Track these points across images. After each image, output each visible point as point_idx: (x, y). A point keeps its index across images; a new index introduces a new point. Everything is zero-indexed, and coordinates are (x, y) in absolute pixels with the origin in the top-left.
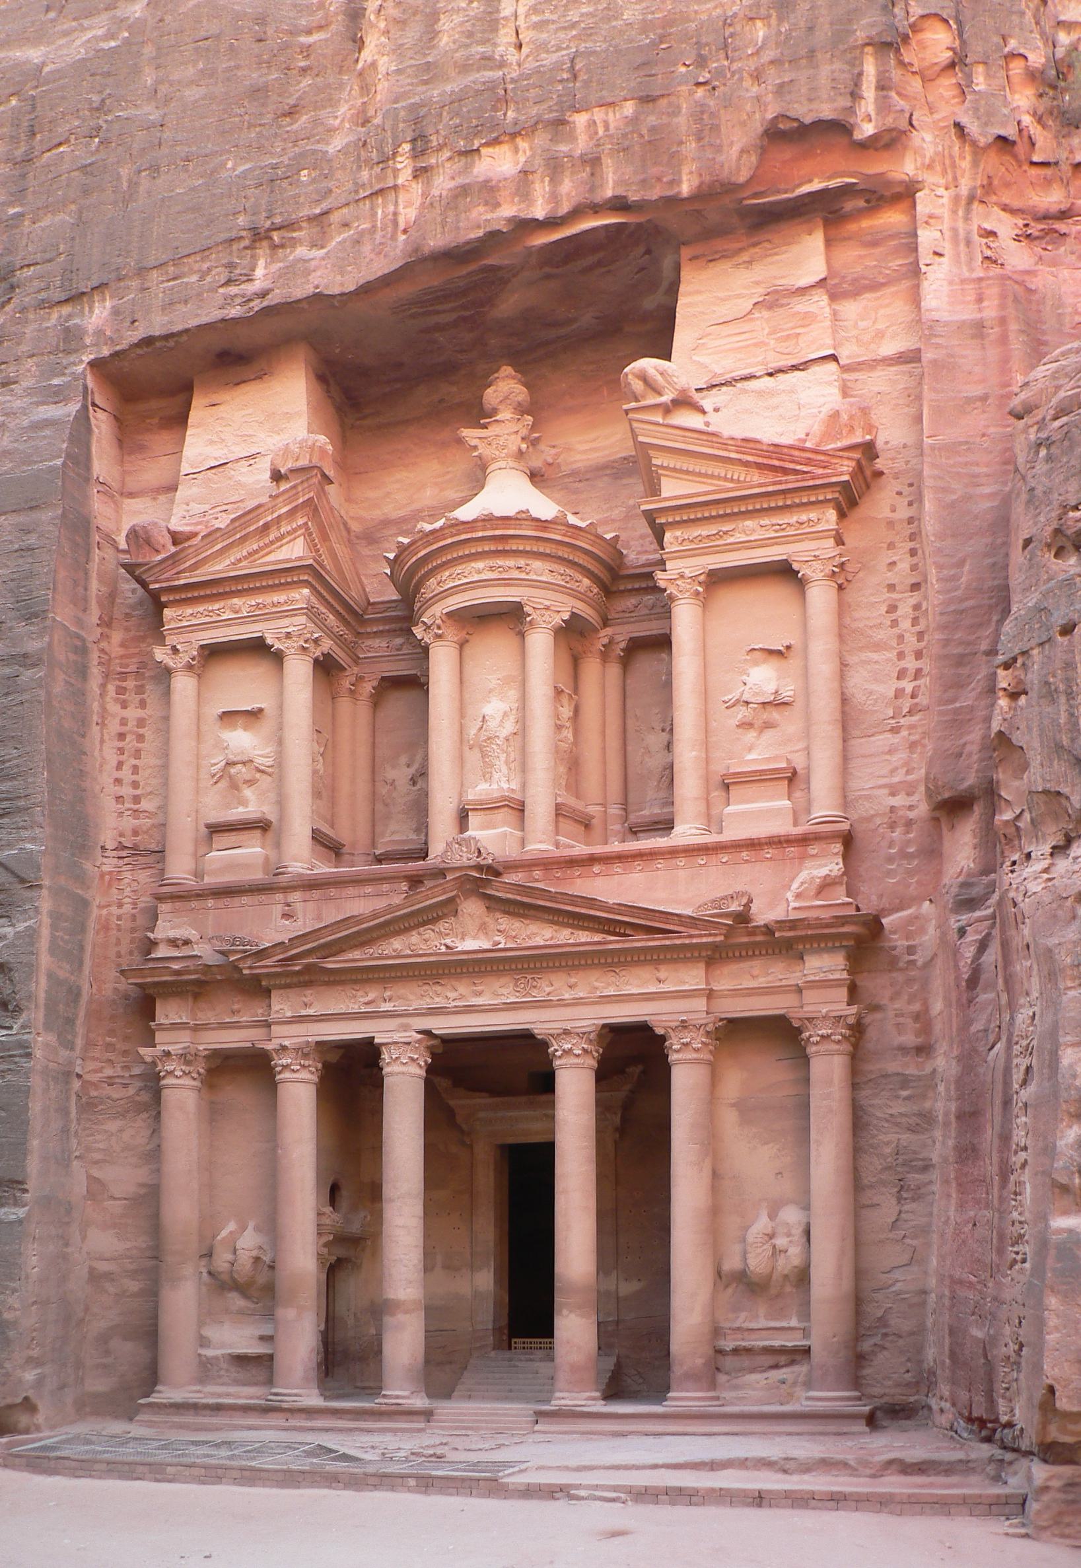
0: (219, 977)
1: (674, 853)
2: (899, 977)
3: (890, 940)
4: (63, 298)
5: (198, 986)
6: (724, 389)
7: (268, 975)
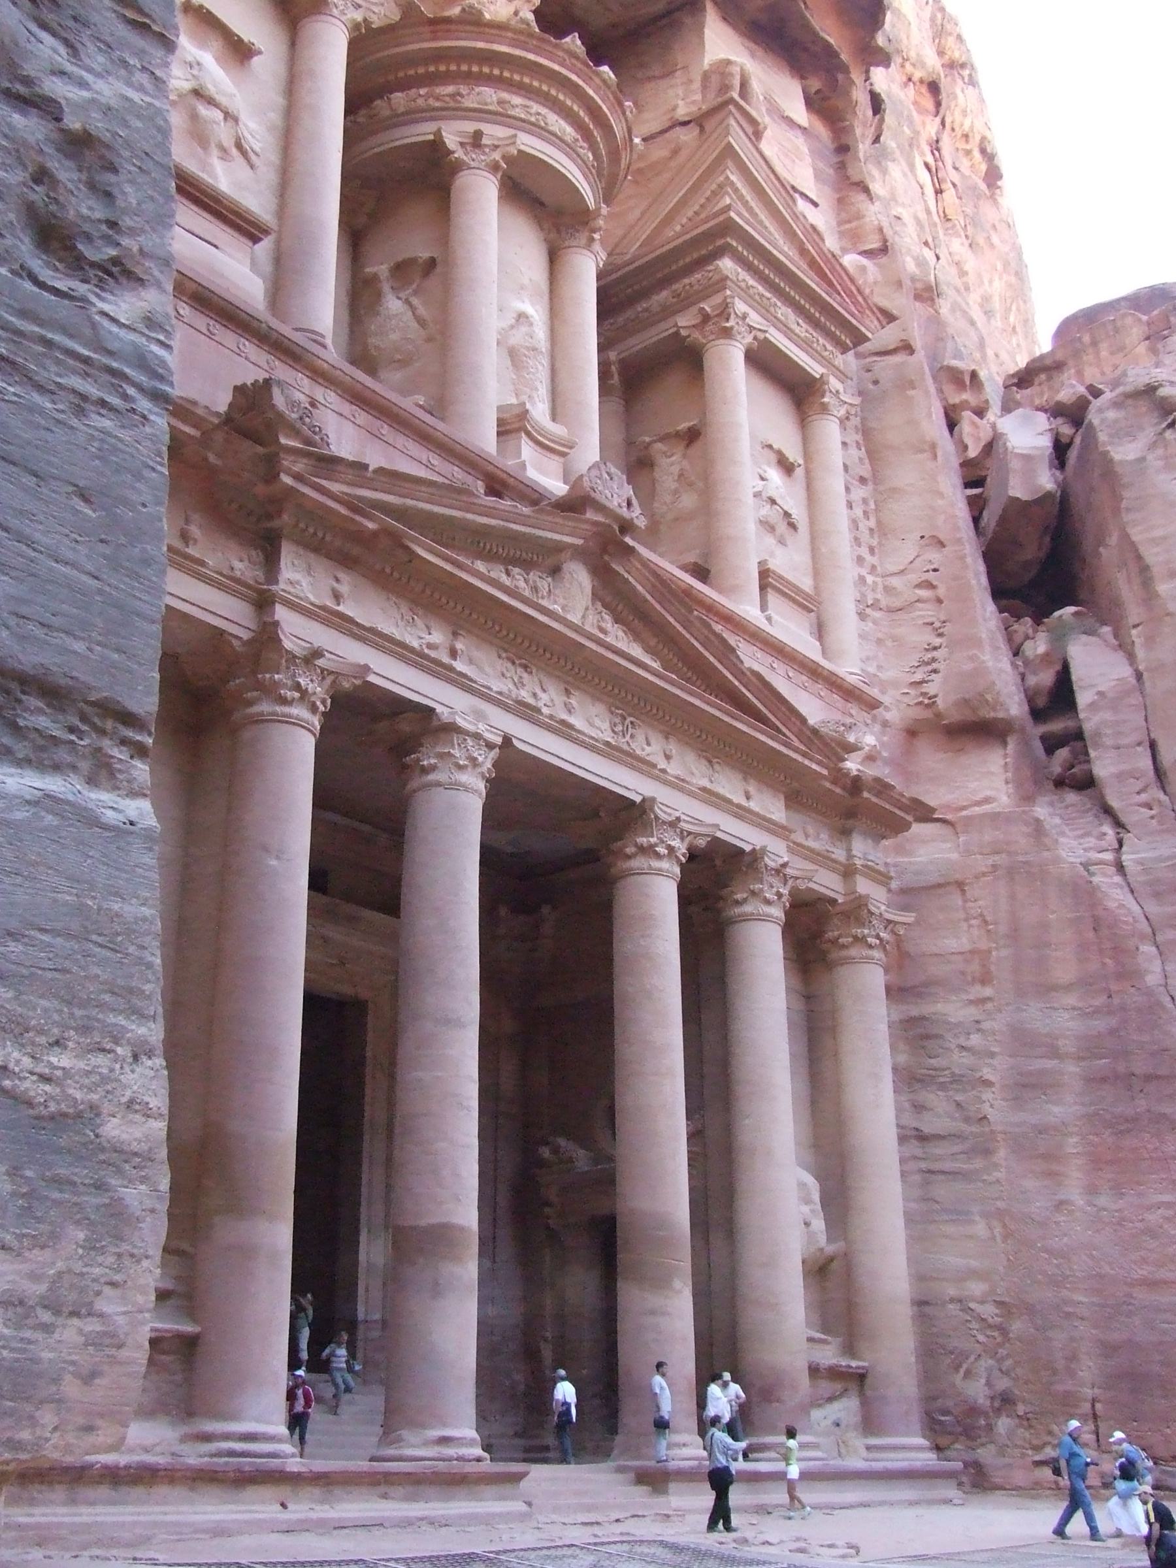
0: (212, 458)
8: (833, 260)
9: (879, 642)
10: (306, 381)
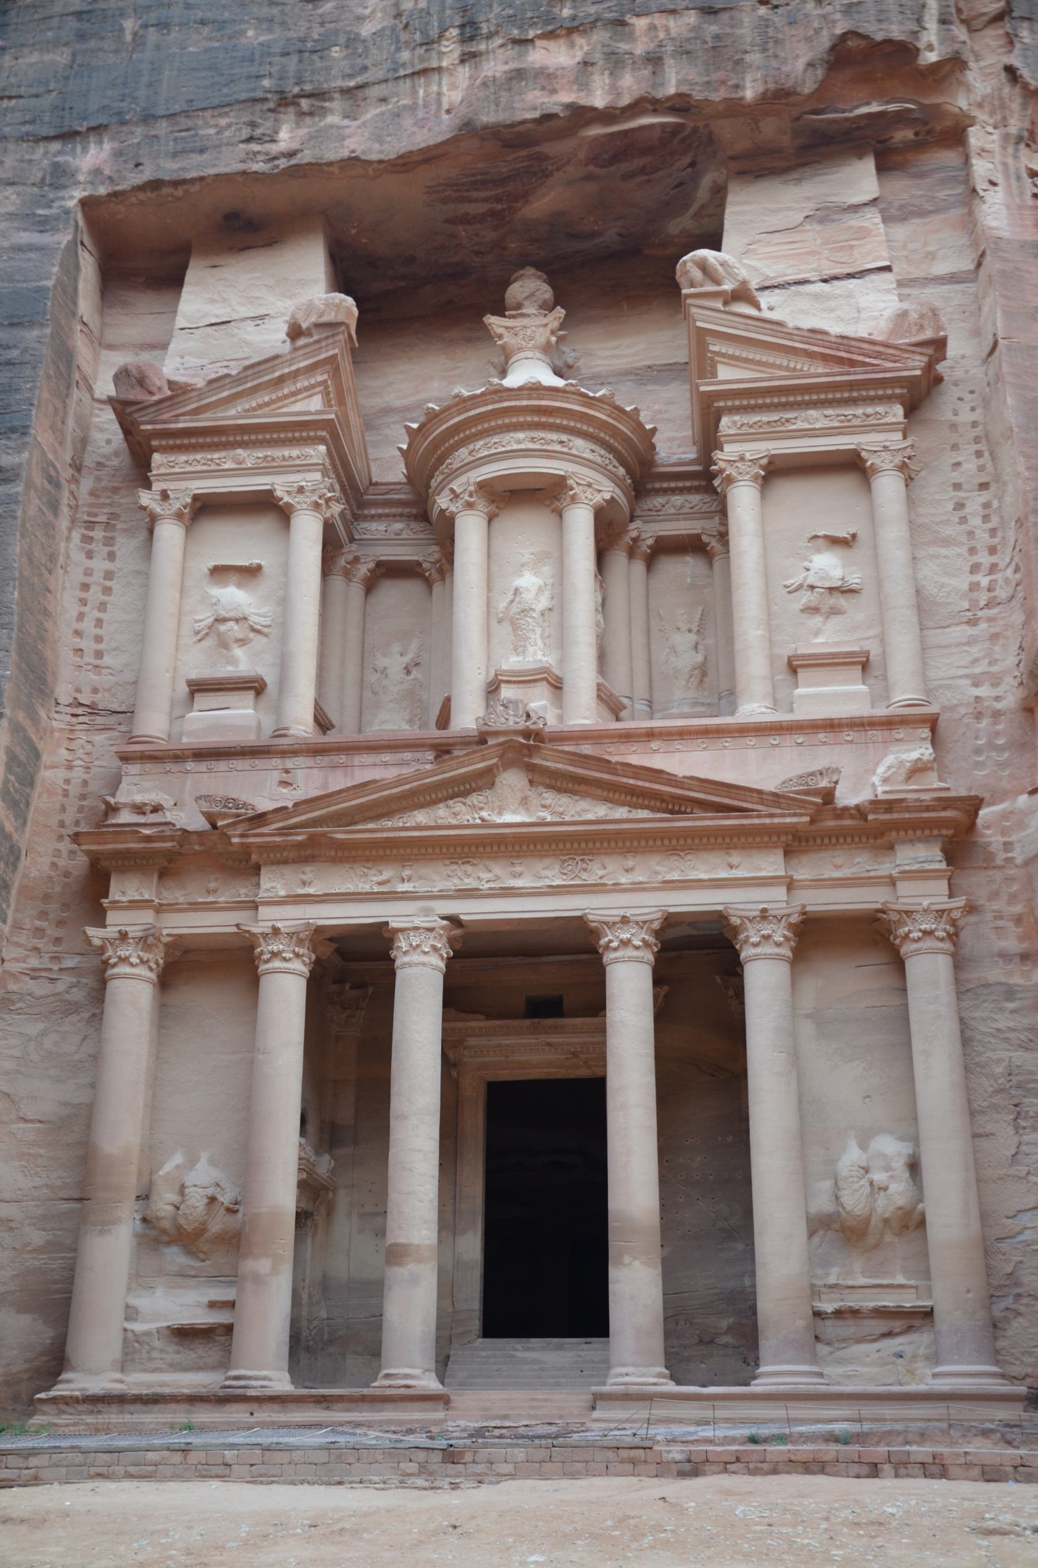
0: (197, 847)
1: (743, 731)
2: (998, 875)
3: (983, 836)
4: (52, 134)
5: (170, 858)
6: (777, 291)
7: (261, 847)
8: (845, 342)
9: (994, 637)
10: (279, 761)
